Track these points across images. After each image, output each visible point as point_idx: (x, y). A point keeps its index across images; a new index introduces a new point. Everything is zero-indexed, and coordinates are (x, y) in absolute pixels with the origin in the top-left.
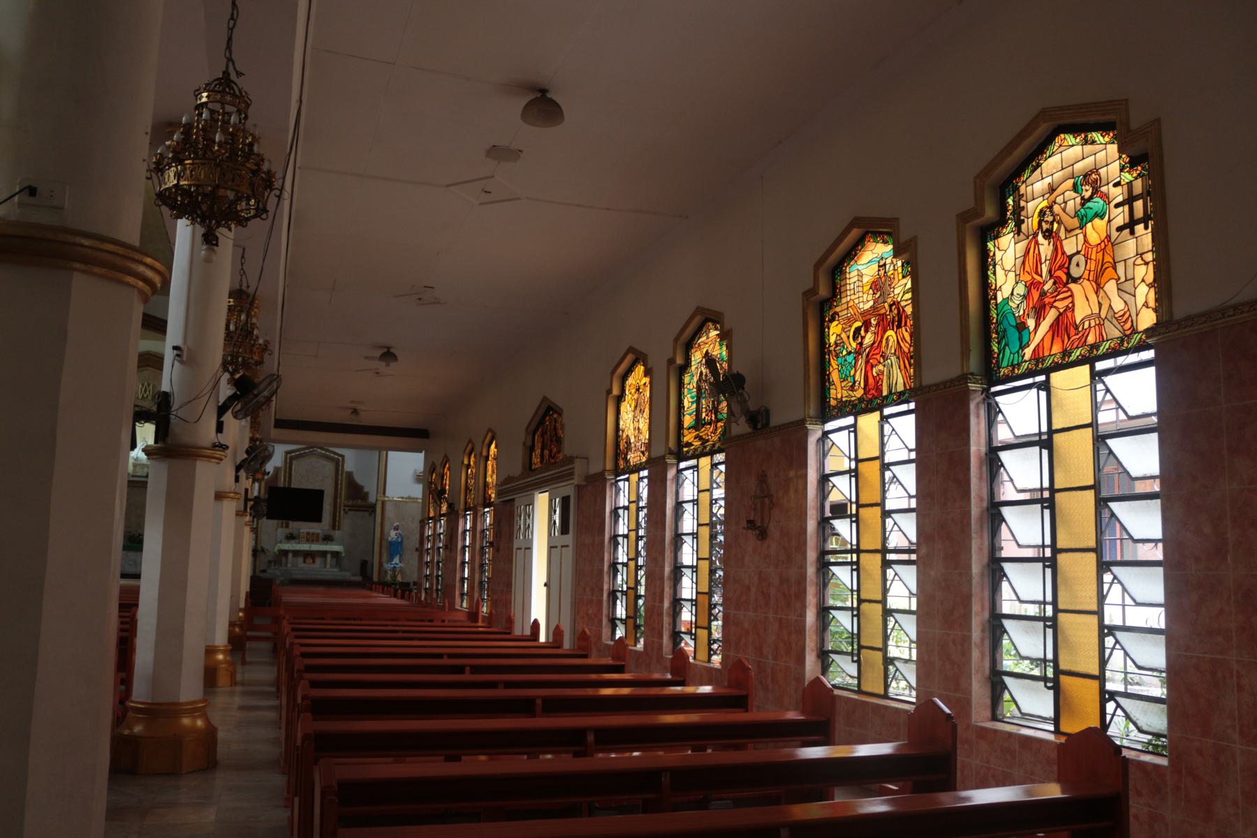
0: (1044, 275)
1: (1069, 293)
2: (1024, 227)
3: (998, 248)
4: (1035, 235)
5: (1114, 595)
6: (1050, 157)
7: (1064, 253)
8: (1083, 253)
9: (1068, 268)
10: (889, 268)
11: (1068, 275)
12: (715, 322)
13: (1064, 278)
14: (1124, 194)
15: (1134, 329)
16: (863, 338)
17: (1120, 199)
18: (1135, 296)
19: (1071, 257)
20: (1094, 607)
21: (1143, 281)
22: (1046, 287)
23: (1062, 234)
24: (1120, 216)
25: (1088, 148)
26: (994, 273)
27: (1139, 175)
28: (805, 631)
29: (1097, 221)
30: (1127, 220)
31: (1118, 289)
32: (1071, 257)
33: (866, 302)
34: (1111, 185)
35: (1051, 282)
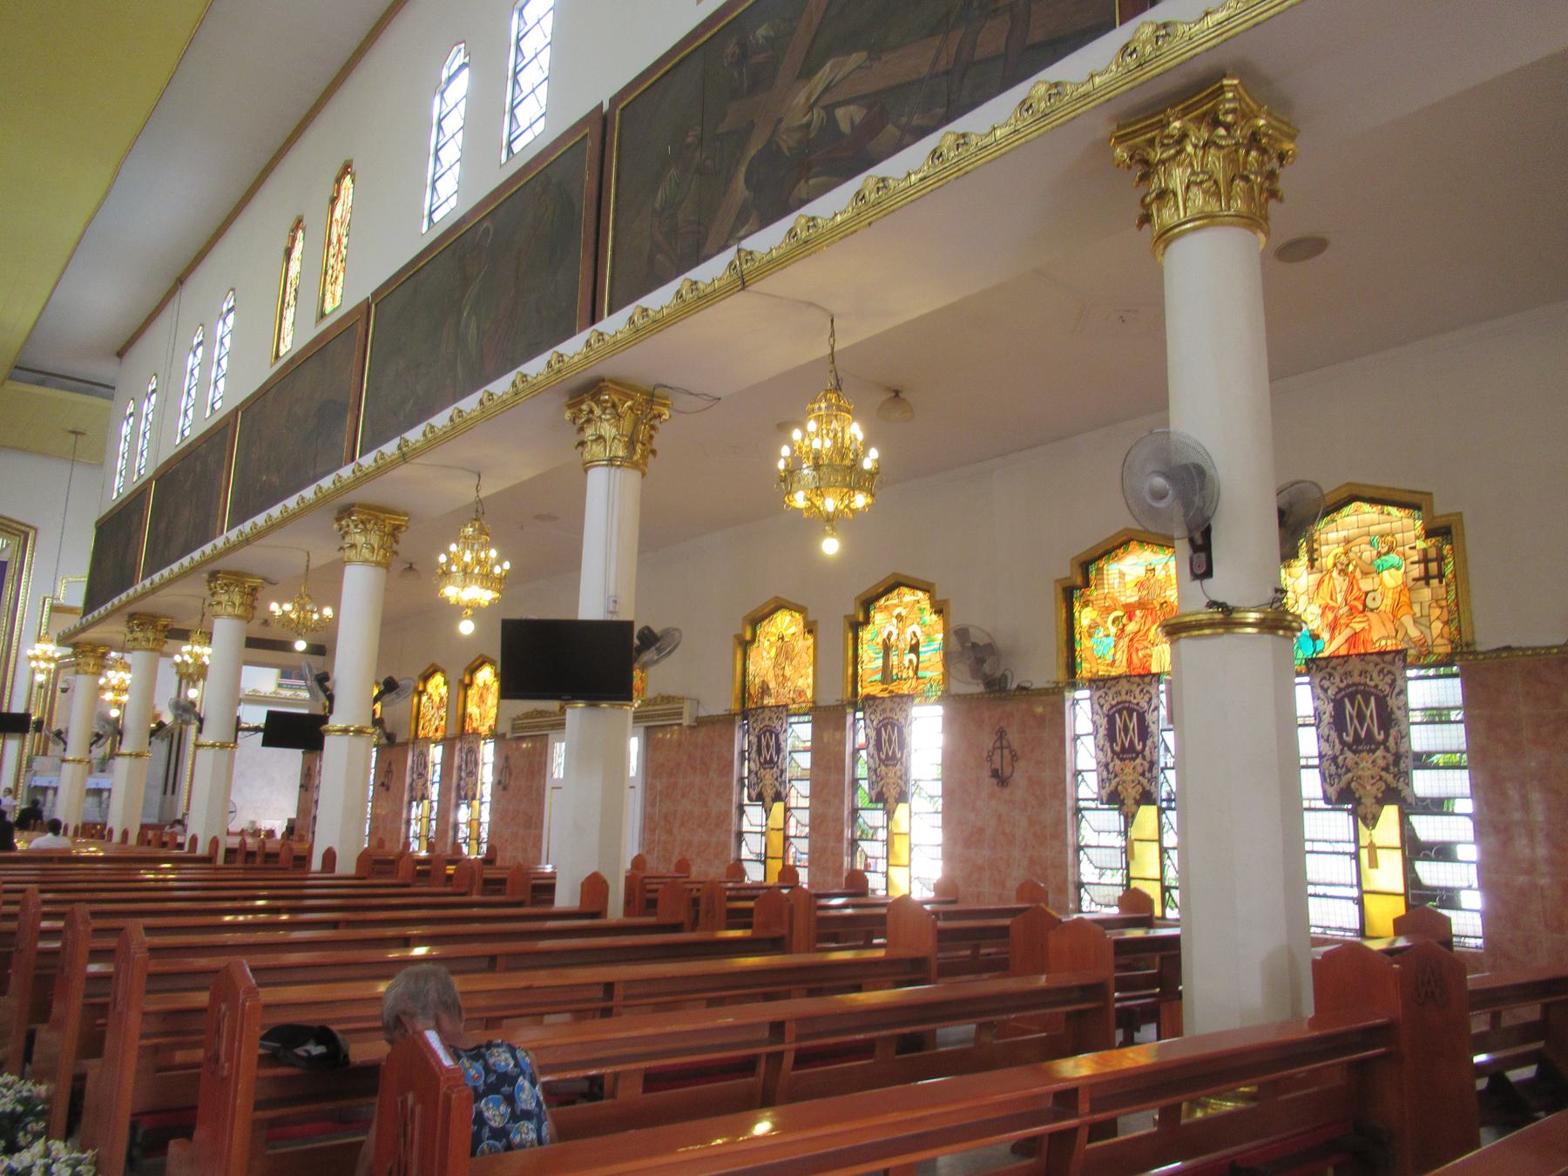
0: (1339, 600)
2: (1317, 564)
4: (1330, 572)
7: (1359, 589)
8: (1379, 591)
9: (1365, 600)
10: (1160, 574)
11: (1365, 606)
16: (1124, 626)
17: (1416, 558)
19: (1367, 594)
21: (1438, 618)
22: (1341, 612)
23: (1358, 574)
24: (1417, 571)
29: (1393, 571)
30: (1423, 574)
32: (1367, 594)
34: (1407, 547)
35: (1347, 608)
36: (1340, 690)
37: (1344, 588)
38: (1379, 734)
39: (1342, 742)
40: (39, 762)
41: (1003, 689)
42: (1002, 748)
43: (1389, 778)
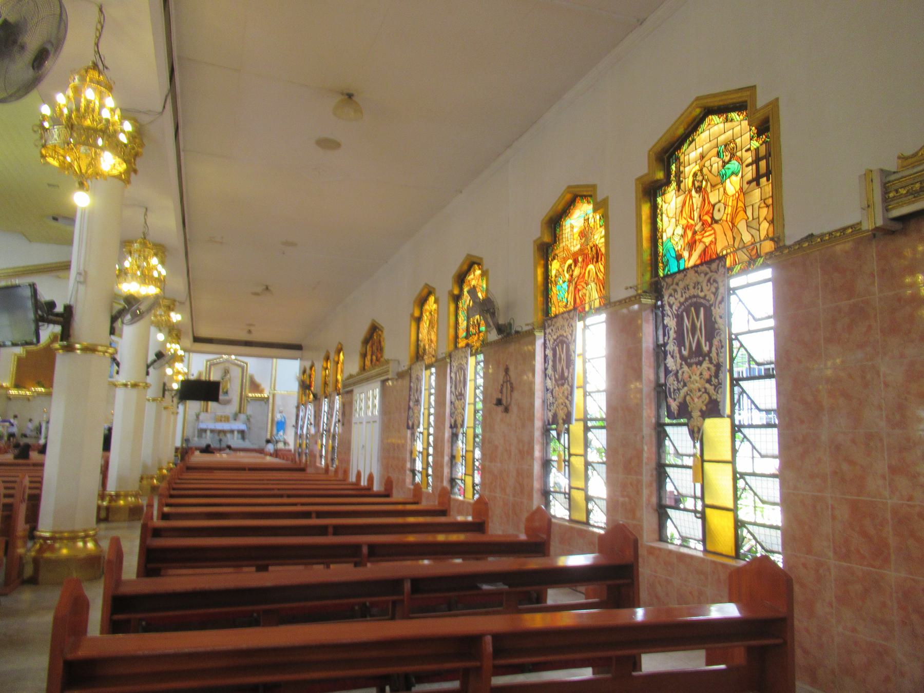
0: (695, 219)
1: (713, 232)
2: (682, 185)
3: (665, 202)
4: (690, 191)
5: (744, 449)
6: (701, 133)
7: (709, 203)
8: (723, 201)
9: (712, 214)
10: (591, 221)
11: (712, 218)
12: (479, 264)
13: (709, 220)
14: (753, 156)
15: (758, 255)
16: (573, 271)
17: (750, 160)
18: (759, 231)
19: (714, 206)
20: (729, 458)
21: (765, 219)
23: (709, 189)
24: (750, 173)
25: (728, 125)
26: (662, 220)
27: (763, 142)
28: (533, 476)
29: (733, 178)
30: (754, 176)
31: (747, 226)
33: (575, 247)
34: (744, 150)
35: (701, 223)
36: (681, 304)
37: (699, 206)
38: (706, 346)
39: (682, 357)
40: (203, 416)
41: (509, 334)
42: (507, 381)
43: (710, 388)
